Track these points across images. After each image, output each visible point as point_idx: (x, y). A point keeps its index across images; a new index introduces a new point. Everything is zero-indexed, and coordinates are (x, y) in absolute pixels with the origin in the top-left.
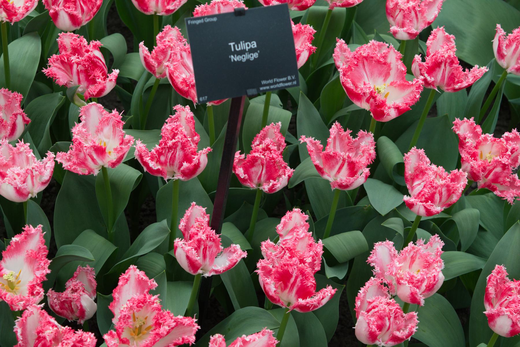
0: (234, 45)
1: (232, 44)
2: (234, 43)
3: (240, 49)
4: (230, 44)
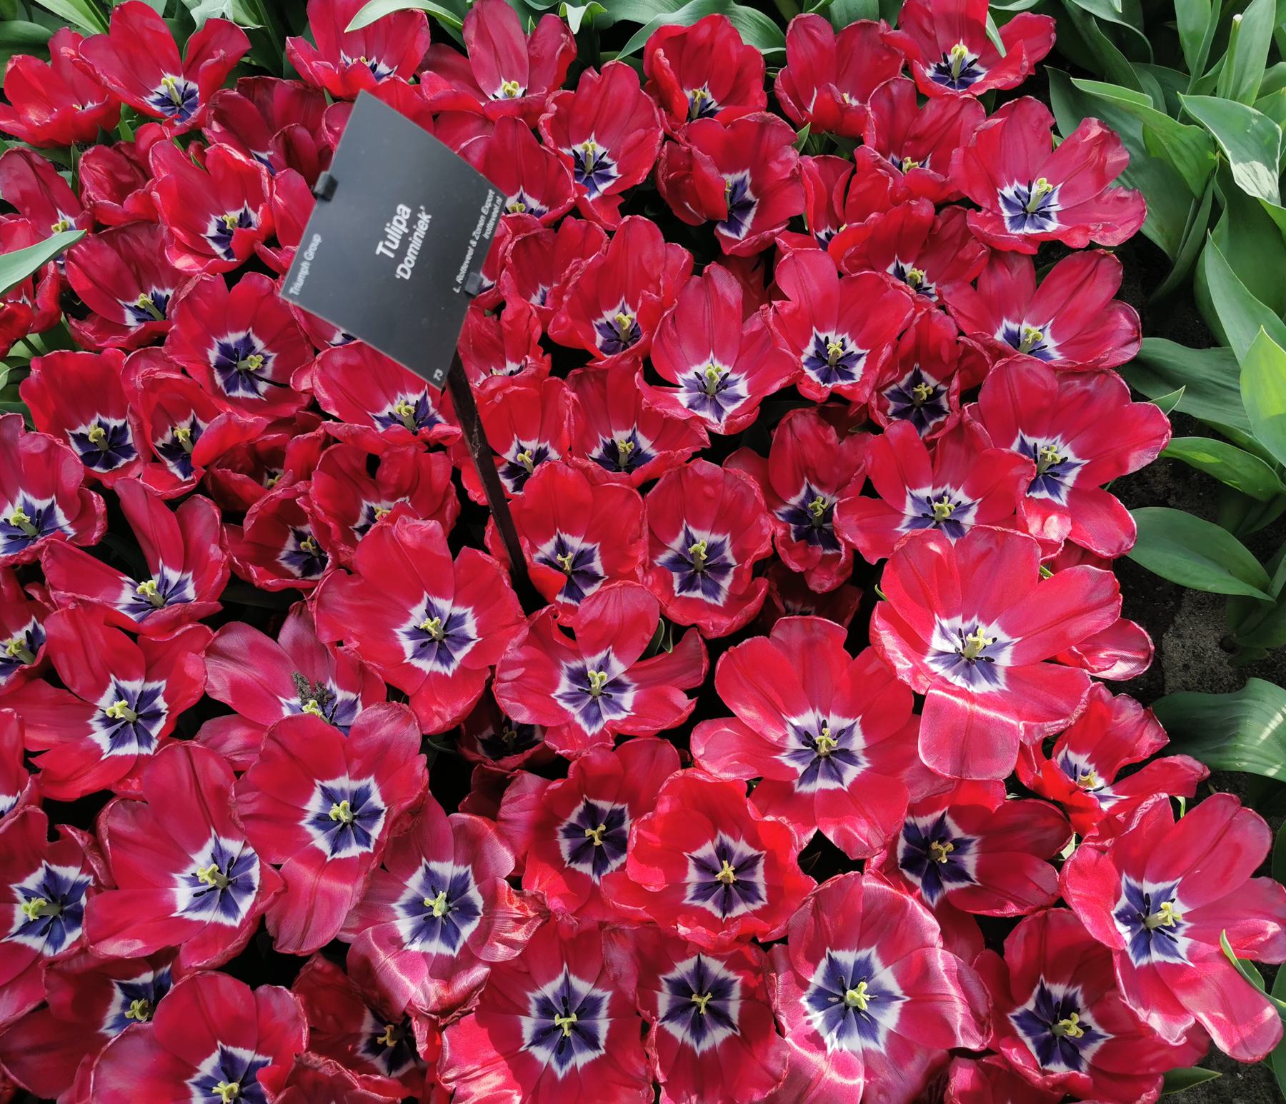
0: (385, 246)
1: (380, 249)
2: (381, 244)
3: (397, 242)
4: (378, 252)
